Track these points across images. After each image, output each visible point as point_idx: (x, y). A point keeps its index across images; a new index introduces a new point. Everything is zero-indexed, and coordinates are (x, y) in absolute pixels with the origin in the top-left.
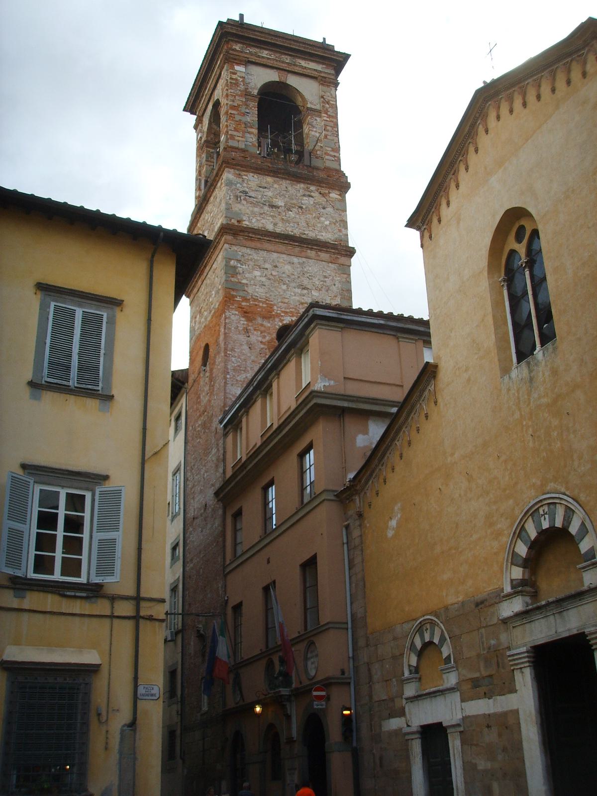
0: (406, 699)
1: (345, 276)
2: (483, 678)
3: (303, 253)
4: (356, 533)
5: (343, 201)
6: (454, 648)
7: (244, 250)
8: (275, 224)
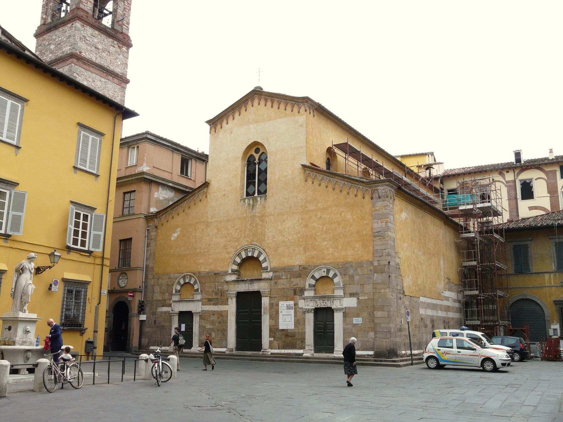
0: (173, 301)
1: (123, 93)
2: (214, 299)
3: (107, 77)
4: (153, 234)
5: (128, 53)
6: (201, 287)
7: (81, 69)
8: (96, 58)
